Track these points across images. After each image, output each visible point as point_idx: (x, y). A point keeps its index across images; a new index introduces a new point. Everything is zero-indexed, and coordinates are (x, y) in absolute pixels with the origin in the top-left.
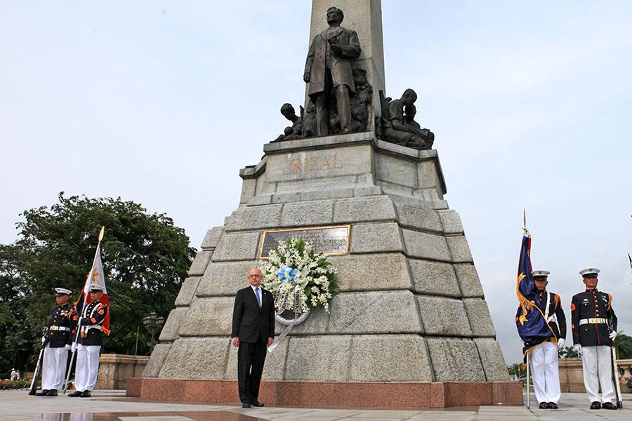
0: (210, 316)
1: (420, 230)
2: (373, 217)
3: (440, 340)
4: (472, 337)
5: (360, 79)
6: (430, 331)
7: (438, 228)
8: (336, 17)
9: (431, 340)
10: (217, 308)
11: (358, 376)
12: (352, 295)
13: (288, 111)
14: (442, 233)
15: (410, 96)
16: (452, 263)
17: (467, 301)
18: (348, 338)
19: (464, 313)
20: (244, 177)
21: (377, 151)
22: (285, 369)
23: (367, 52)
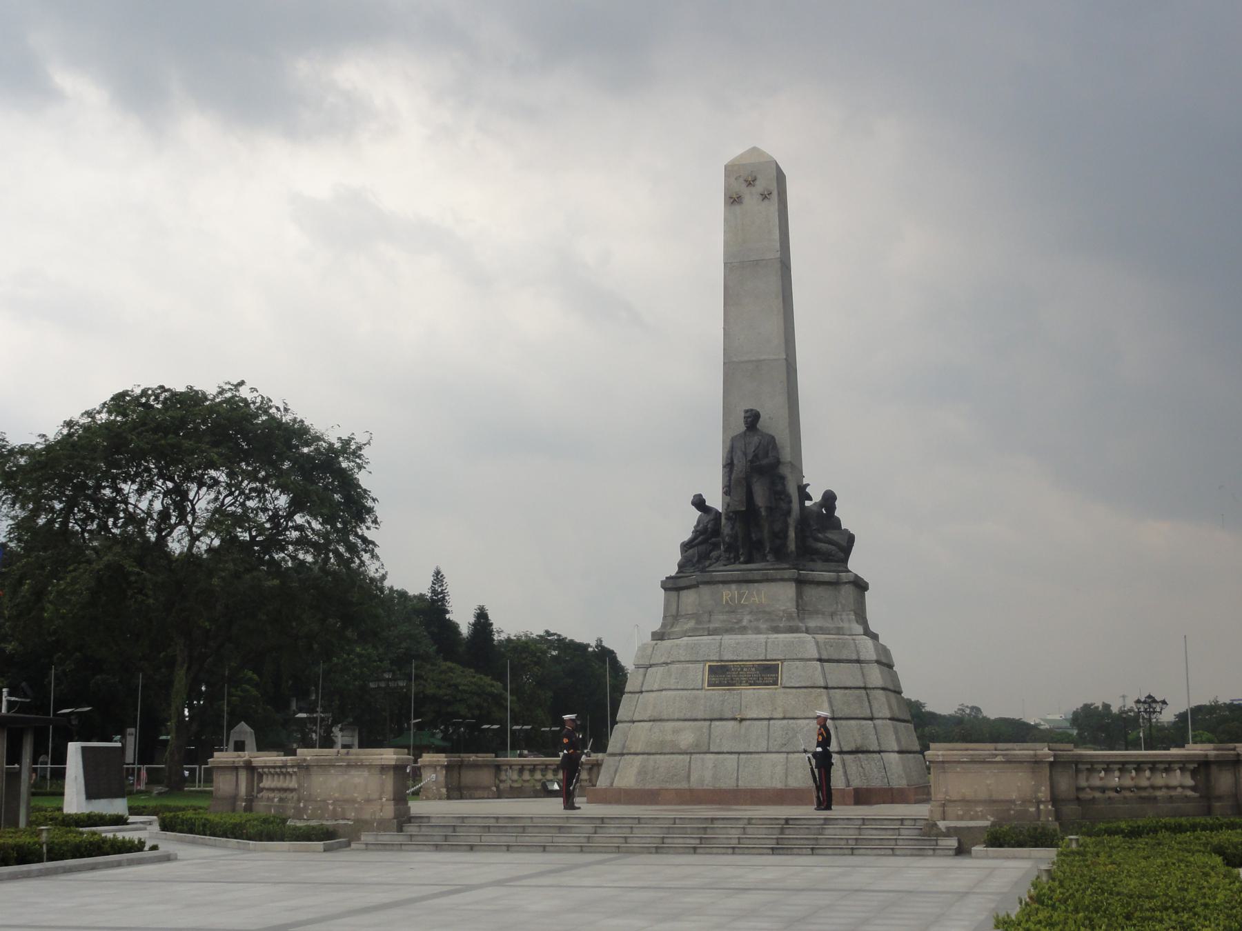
0: (669, 738)
1: (838, 661)
2: (800, 656)
3: (852, 756)
4: (879, 752)
5: (779, 488)
6: (845, 749)
7: (854, 657)
8: (752, 419)
9: (846, 757)
10: (676, 731)
12: (785, 722)
13: (699, 503)
14: (858, 661)
15: (829, 499)
16: (865, 688)
17: (877, 722)
18: (784, 755)
19: (873, 732)
20: (666, 589)
21: (800, 582)
22: (737, 779)
23: (786, 455)
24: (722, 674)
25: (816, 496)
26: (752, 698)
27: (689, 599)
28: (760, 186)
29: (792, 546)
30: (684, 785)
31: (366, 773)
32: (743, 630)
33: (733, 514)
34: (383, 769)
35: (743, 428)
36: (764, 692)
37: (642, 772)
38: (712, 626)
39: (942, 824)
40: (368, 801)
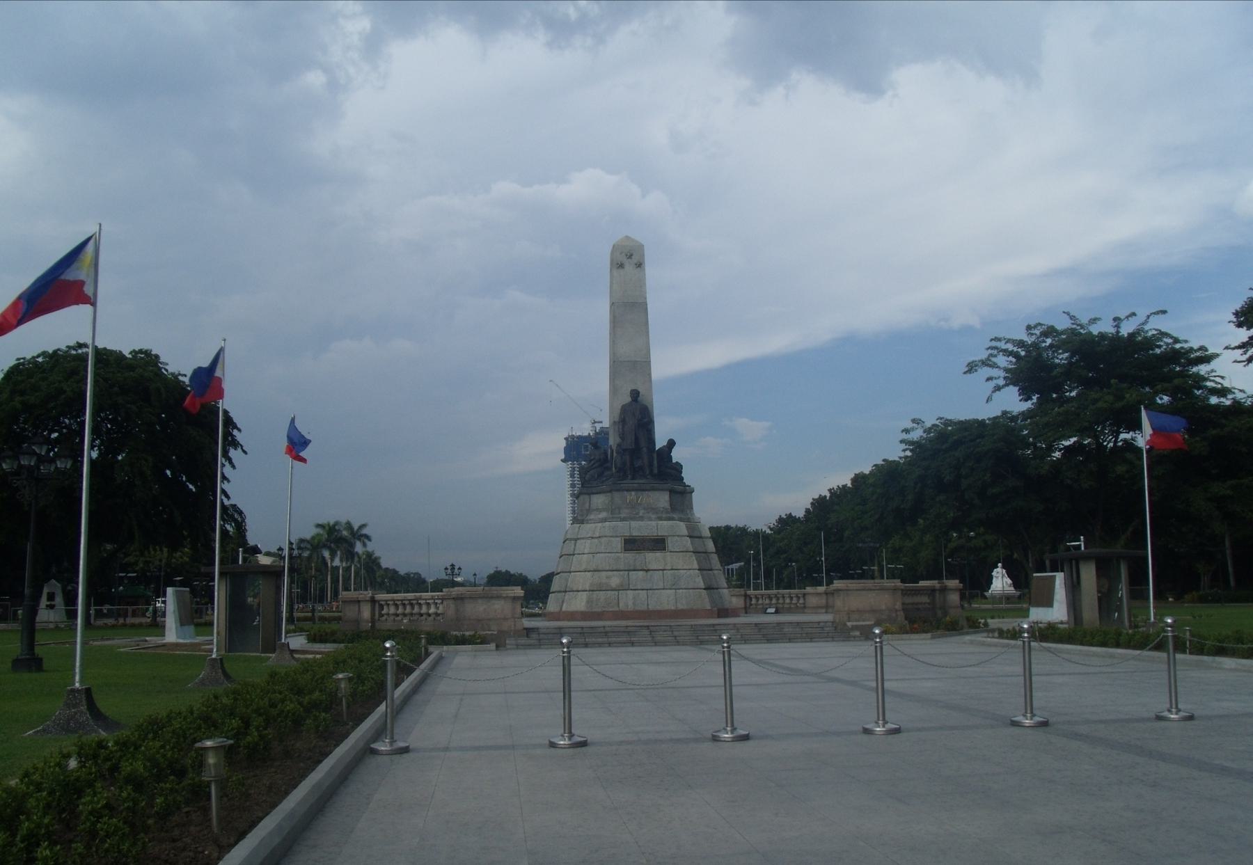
11: (680, 607)
15: (671, 444)
24: (632, 544)
25: (660, 443)
26: (653, 559)
27: (599, 500)
28: (635, 259)
29: (656, 471)
30: (616, 609)
31: (502, 602)
32: (642, 518)
33: (622, 450)
34: (515, 599)
35: (629, 399)
36: (658, 554)
37: (589, 601)
38: (622, 516)
39: (849, 624)
40: (505, 619)
